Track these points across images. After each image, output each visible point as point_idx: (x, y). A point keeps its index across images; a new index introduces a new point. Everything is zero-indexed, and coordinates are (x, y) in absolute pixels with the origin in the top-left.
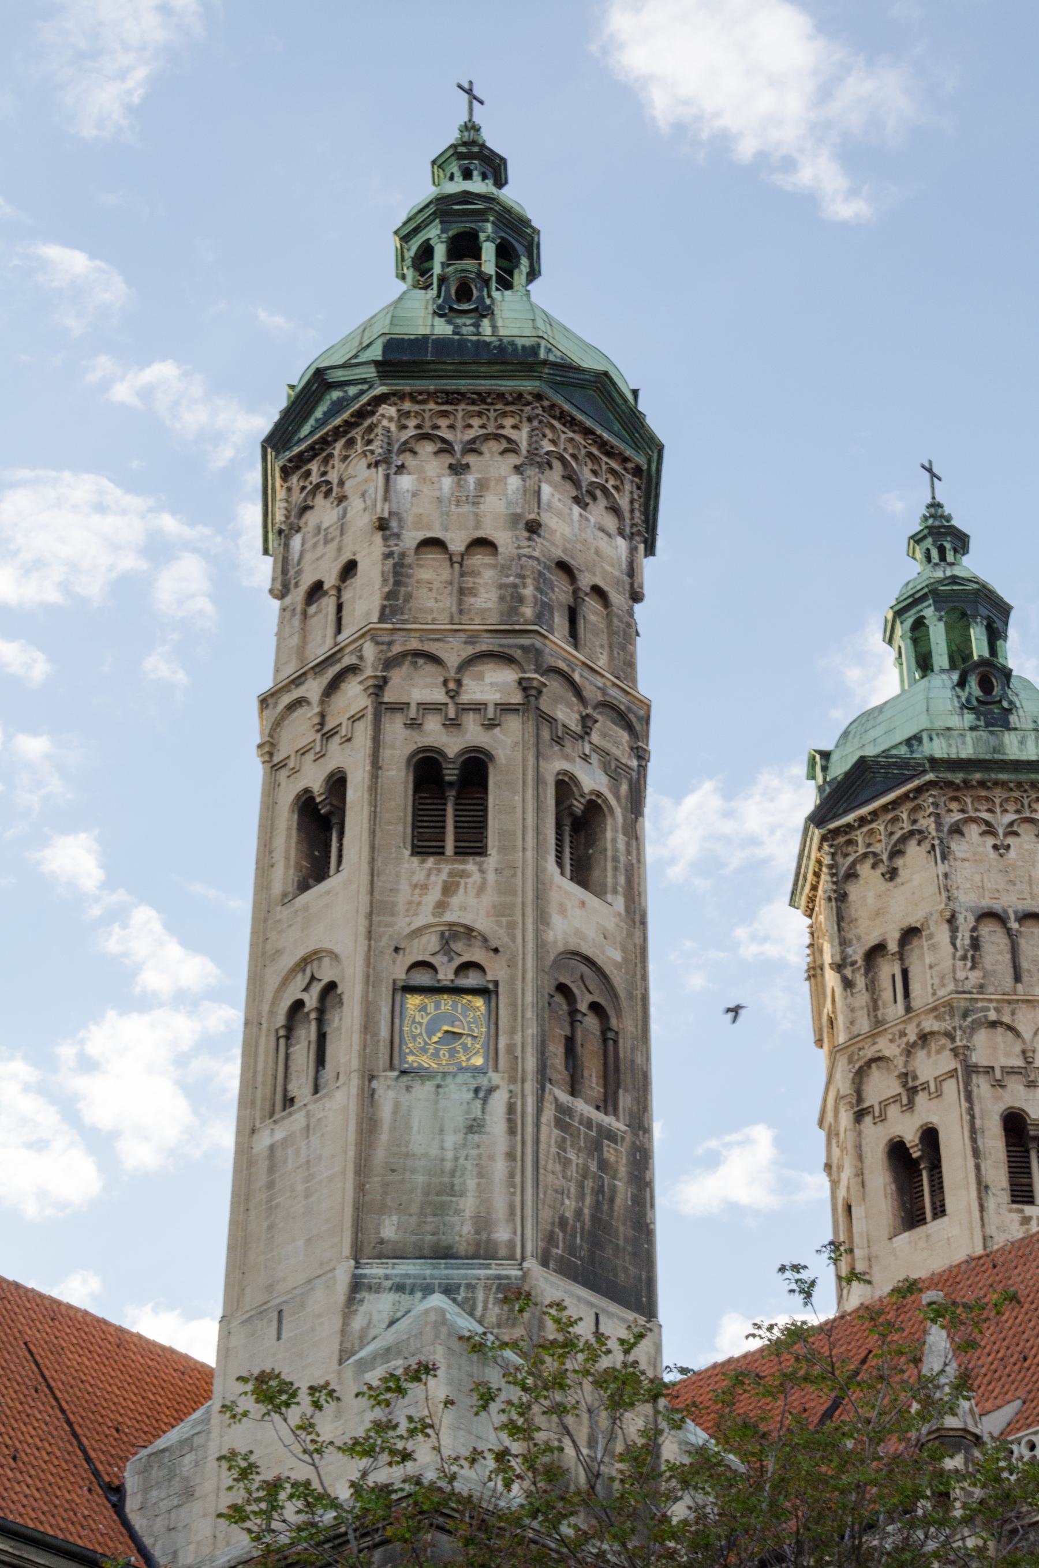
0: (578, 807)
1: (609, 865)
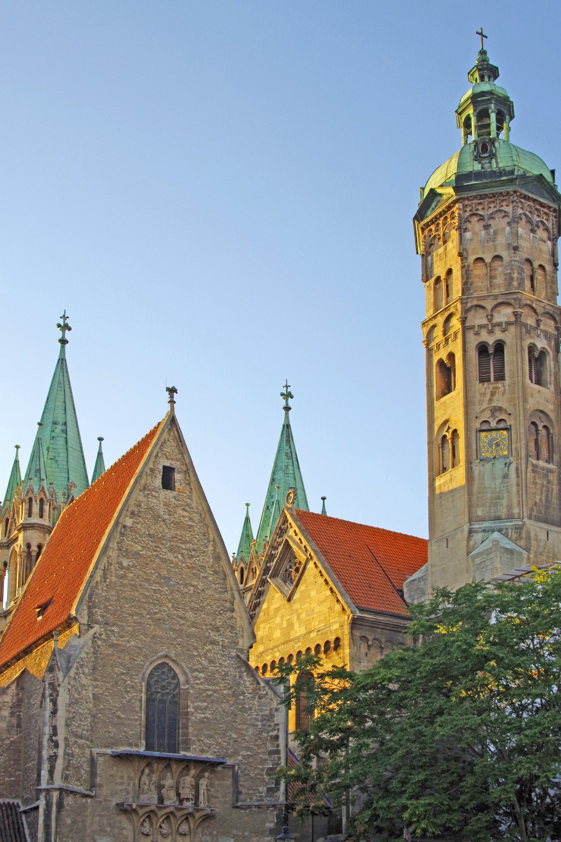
0: (536, 354)
1: (548, 374)
